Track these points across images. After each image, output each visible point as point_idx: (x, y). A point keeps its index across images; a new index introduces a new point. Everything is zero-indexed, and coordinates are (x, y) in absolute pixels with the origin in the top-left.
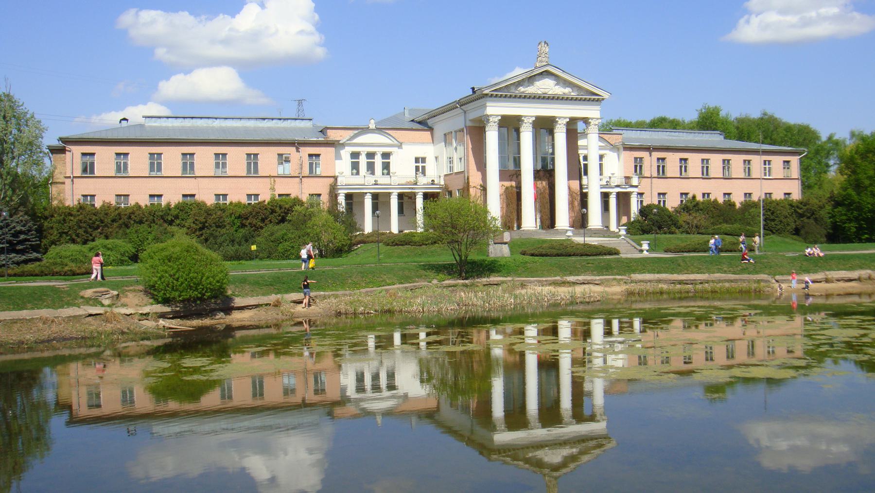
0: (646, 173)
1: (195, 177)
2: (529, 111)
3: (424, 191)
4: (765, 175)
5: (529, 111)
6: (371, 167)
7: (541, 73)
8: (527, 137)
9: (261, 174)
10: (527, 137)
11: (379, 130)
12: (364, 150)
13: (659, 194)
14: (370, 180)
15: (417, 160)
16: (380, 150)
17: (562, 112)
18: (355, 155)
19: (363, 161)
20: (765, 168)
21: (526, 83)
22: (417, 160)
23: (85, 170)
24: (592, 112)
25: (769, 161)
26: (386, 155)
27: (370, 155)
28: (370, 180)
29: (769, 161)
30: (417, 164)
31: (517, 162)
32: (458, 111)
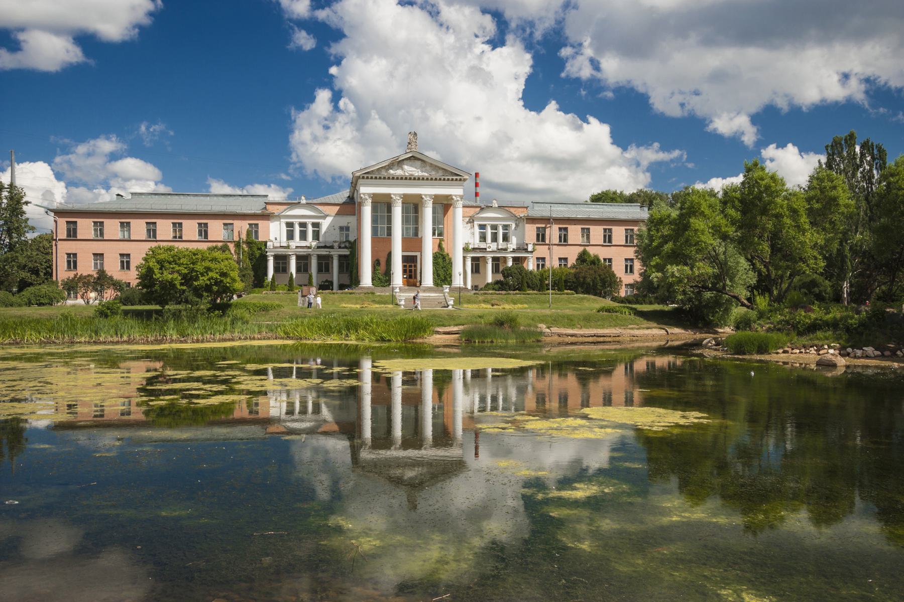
3: (492, 256)
5: (396, 191)
7: (409, 158)
9: (209, 239)
11: (309, 205)
13: (560, 259)
14: (494, 246)
17: (427, 191)
18: (290, 225)
19: (297, 229)
21: (396, 167)
23: (69, 235)
24: (455, 191)
28: (494, 246)
30: (347, 232)
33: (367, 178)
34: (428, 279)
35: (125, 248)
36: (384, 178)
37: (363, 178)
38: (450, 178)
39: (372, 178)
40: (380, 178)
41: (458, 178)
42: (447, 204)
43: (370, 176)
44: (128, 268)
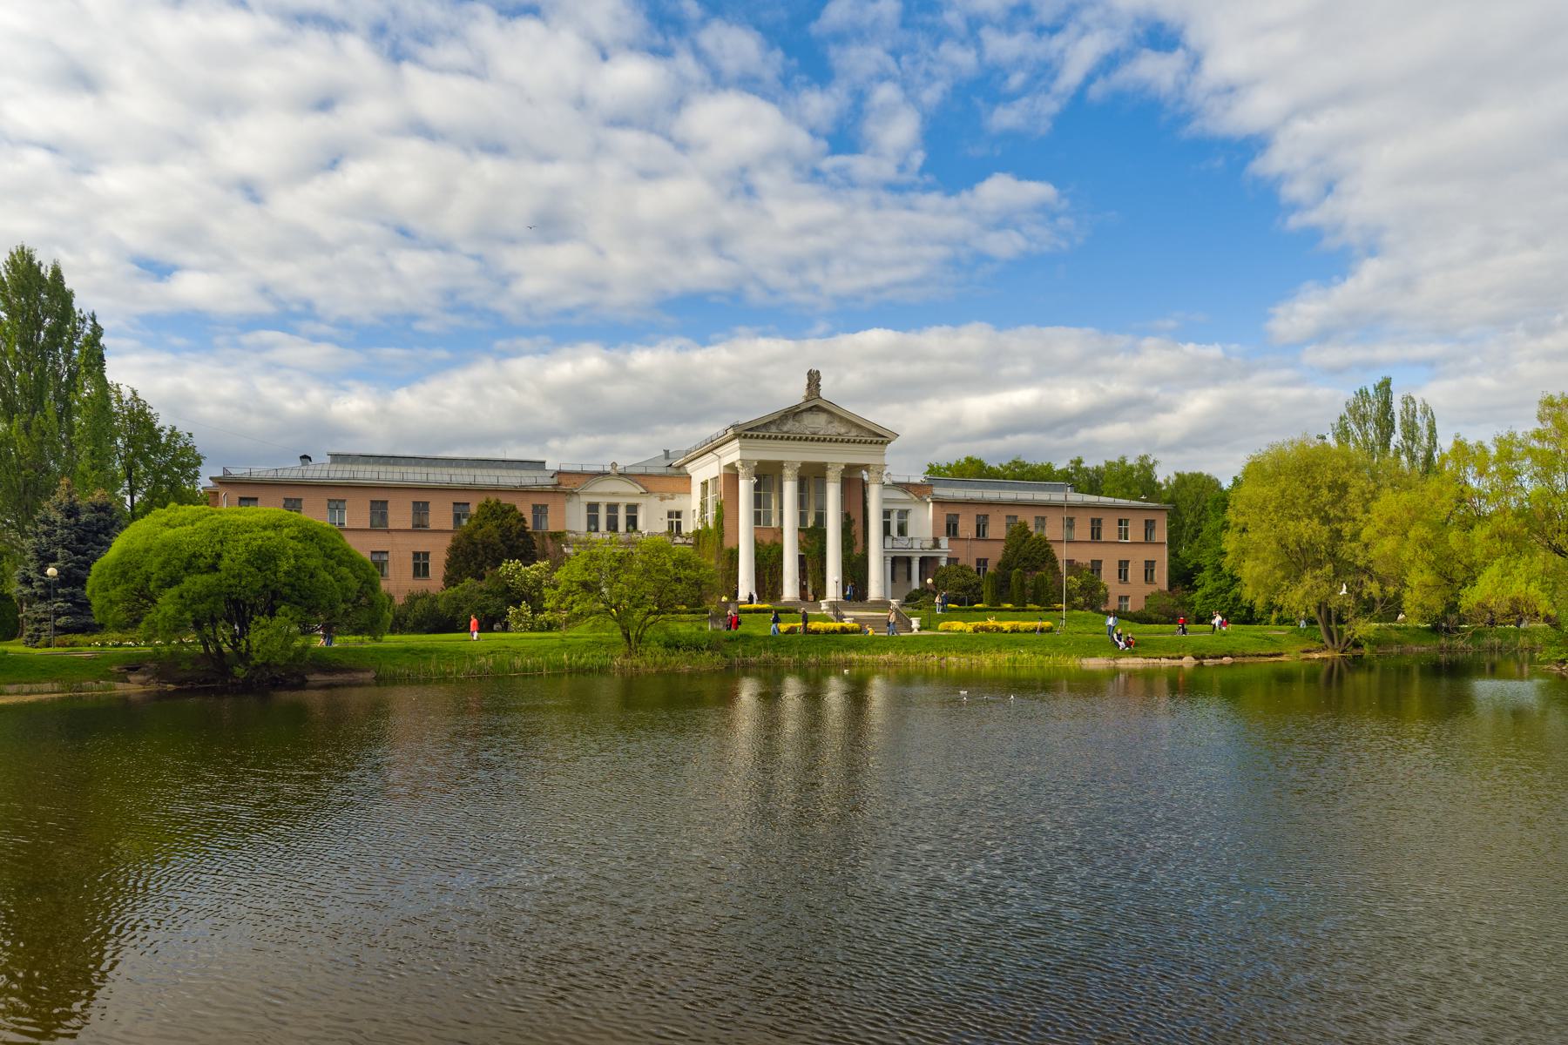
0: (961, 534)
1: (388, 531)
2: (793, 455)
4: (1120, 537)
5: (793, 455)
6: (612, 525)
7: (810, 409)
8: (790, 489)
10: (790, 489)
12: (603, 501)
15: (670, 515)
16: (623, 502)
18: (593, 508)
20: (1120, 530)
22: (670, 515)
25: (1126, 520)
26: (632, 509)
27: (613, 508)
29: (1126, 520)
31: (821, 518)
32: (710, 454)
33: (752, 437)
34: (833, 590)
35: (422, 543)
36: (776, 438)
37: (745, 437)
38: (869, 439)
39: (758, 437)
40: (770, 438)
41: (880, 439)
42: (849, 479)
43: (755, 434)
44: (426, 573)
